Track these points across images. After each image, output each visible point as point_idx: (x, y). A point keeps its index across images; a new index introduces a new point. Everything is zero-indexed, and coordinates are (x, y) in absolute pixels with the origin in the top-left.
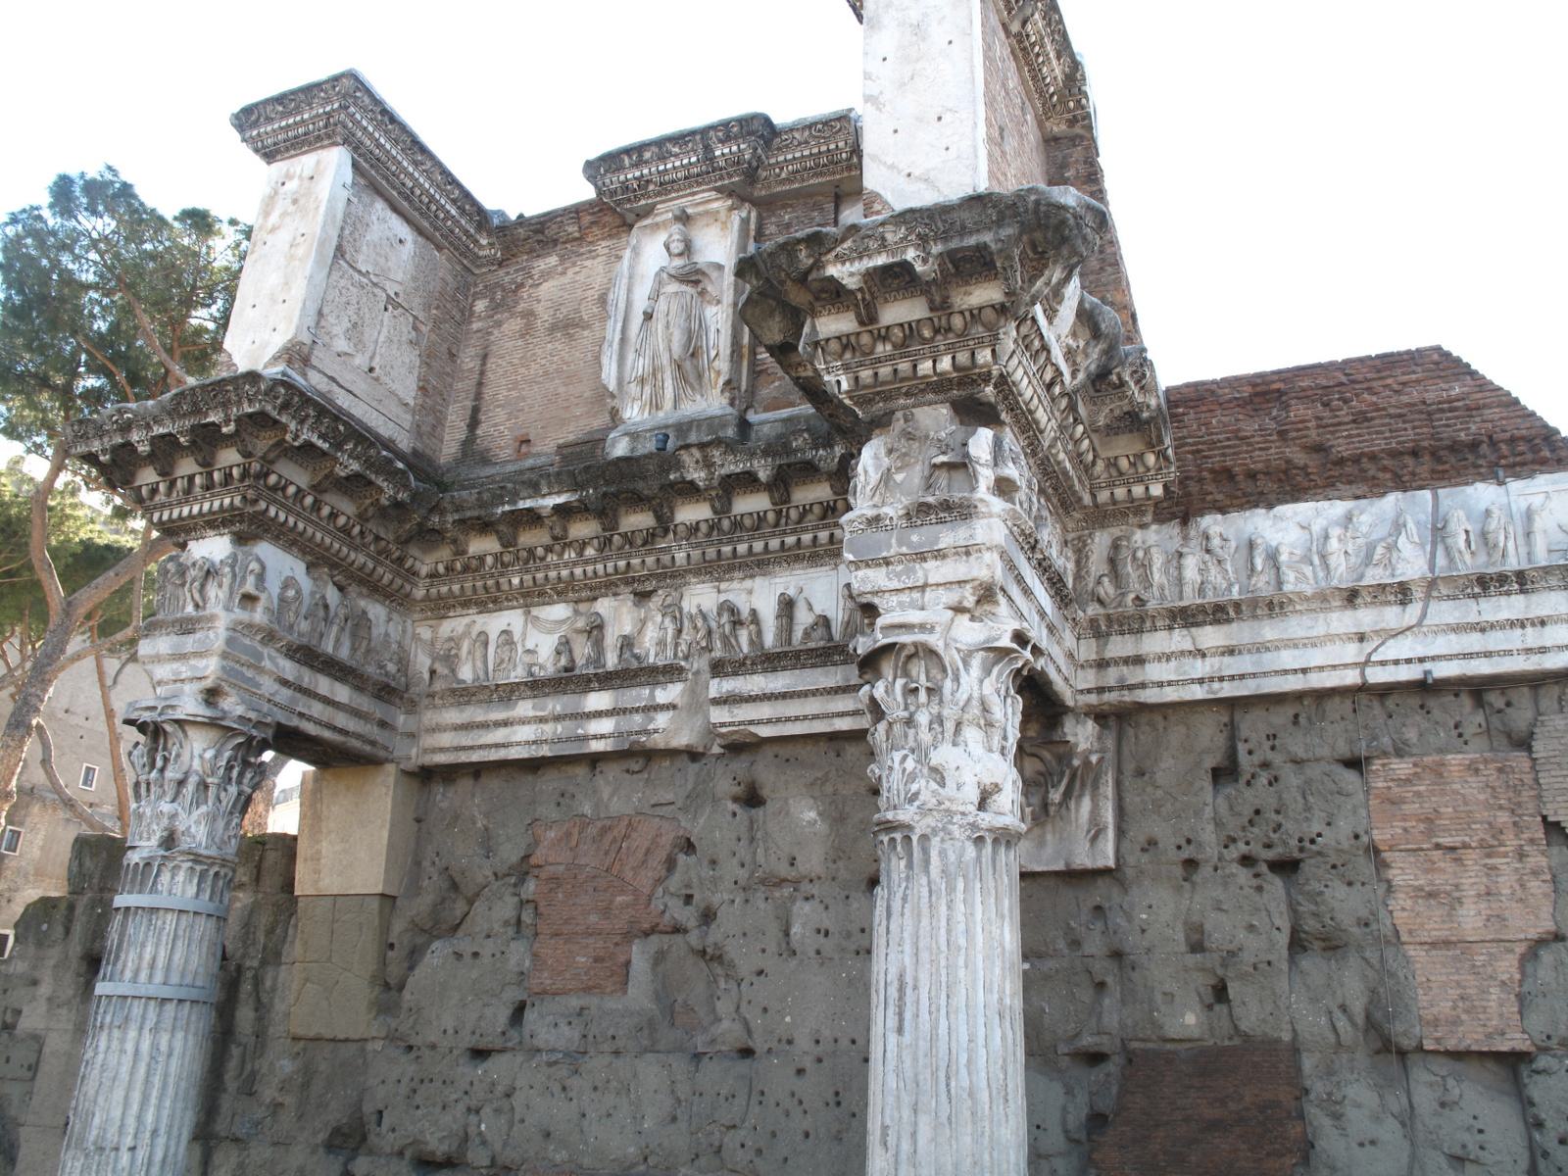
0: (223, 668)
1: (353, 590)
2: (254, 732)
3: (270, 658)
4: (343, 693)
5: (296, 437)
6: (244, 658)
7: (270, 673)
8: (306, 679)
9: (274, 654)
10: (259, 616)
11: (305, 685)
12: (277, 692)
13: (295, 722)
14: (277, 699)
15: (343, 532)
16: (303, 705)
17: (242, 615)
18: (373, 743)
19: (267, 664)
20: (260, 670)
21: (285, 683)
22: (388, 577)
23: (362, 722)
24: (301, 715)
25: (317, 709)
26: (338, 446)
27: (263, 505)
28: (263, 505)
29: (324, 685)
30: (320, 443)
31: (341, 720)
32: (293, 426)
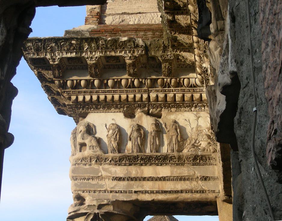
0: (76, 185)
1: (164, 112)
2: (97, 211)
3: (104, 169)
4: (164, 171)
5: (54, 60)
6: (87, 175)
7: (108, 178)
8: (134, 172)
9: (106, 166)
10: (87, 152)
11: (133, 176)
12: (116, 185)
13: (134, 197)
14: (117, 189)
15: (130, 87)
16: (136, 186)
17: (79, 155)
18: (202, 192)
19: (104, 174)
20: (101, 178)
21: (120, 179)
22: (178, 96)
23: (187, 182)
24: (136, 192)
25: (148, 186)
26: (80, 49)
27: (74, 98)
28: (74, 98)
29: (148, 171)
30: (69, 55)
31: (169, 186)
32: (48, 56)
